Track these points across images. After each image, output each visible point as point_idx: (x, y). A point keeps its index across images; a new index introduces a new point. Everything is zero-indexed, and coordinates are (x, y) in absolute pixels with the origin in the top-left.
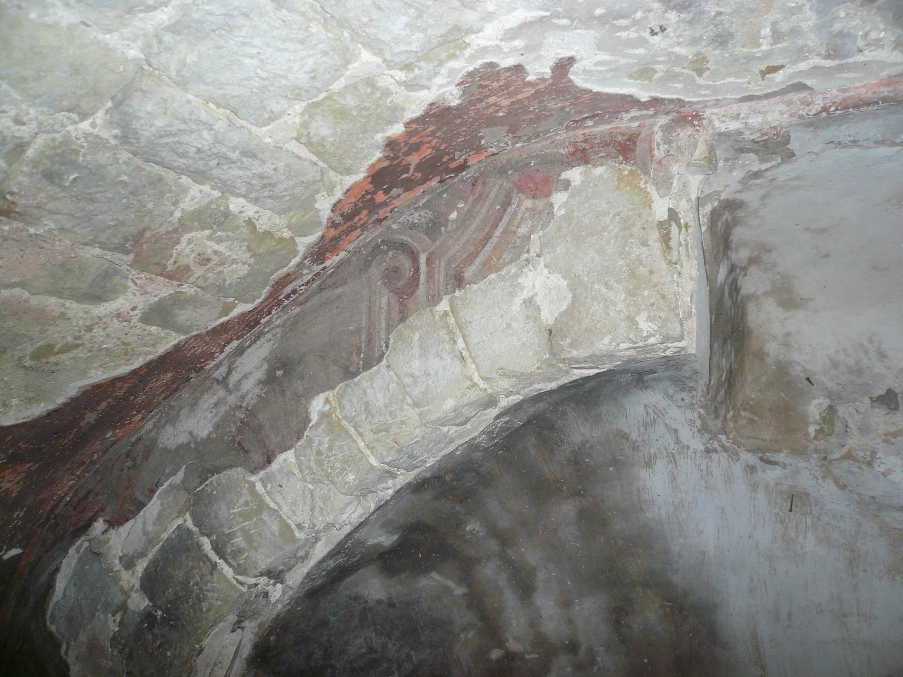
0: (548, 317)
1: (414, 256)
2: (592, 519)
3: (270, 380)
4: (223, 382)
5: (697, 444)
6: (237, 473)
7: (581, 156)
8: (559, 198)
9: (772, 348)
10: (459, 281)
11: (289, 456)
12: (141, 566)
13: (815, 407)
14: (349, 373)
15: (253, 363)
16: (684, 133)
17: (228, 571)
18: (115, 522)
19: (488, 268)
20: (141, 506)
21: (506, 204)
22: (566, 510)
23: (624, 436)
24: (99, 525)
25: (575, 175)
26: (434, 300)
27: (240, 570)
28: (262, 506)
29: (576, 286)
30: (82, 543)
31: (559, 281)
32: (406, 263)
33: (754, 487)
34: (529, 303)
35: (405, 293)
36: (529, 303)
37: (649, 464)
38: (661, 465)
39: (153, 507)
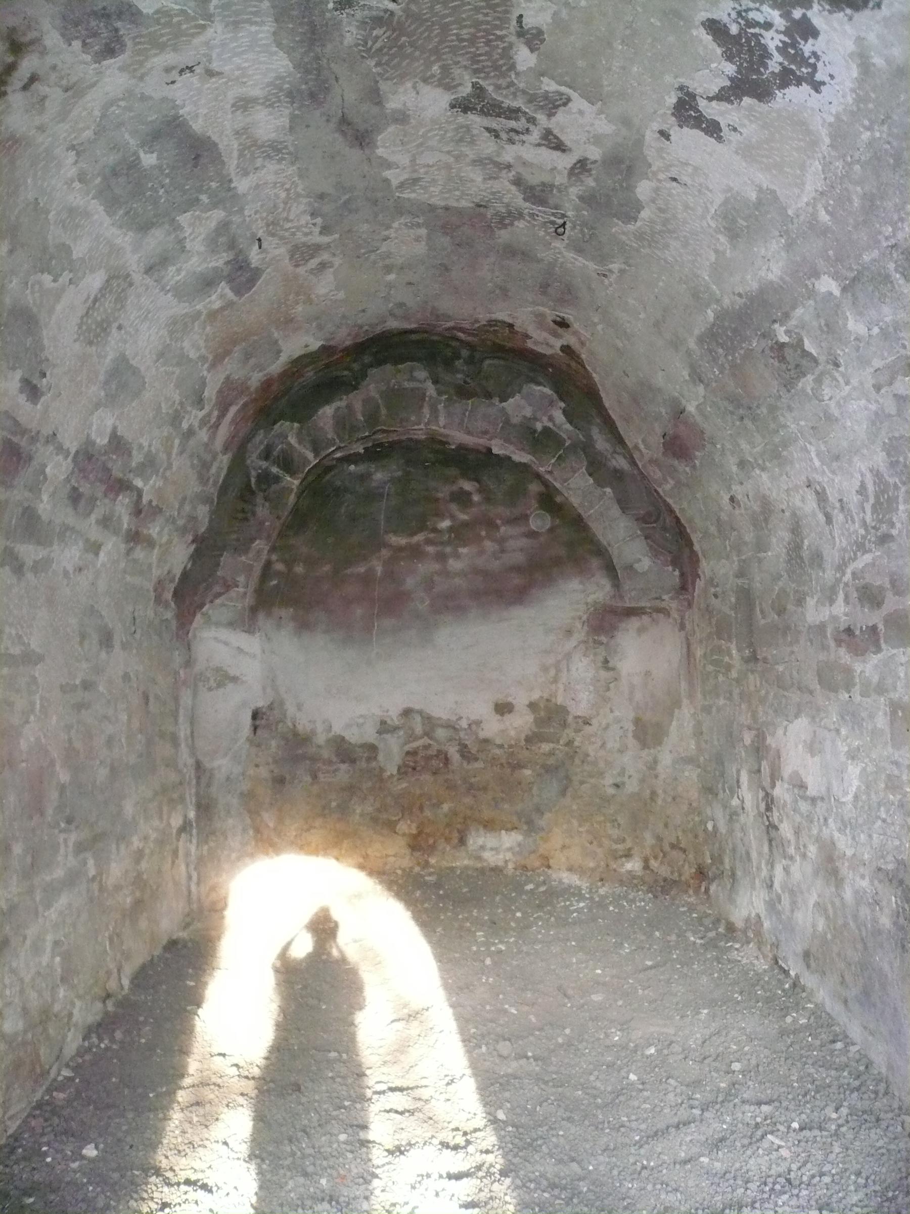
0: (636, 566)
1: (655, 522)
2: (557, 562)
3: (616, 471)
4: (615, 452)
5: (590, 599)
6: (585, 463)
7: (682, 575)
8: (670, 568)
9: (624, 625)
10: (646, 538)
11: (591, 481)
12: (550, 425)
13: (603, 639)
14: (619, 501)
15: (620, 462)
16: (686, 603)
17: (553, 461)
18: (565, 412)
19: (651, 547)
20: (571, 423)
21: (670, 552)
22: (562, 552)
23: (593, 576)
24: (563, 405)
25: (677, 573)
26: (642, 529)
27: (554, 464)
28: (575, 472)
29: (644, 574)
30: (555, 397)
31: (646, 568)
32: (654, 518)
33: (573, 618)
34: (640, 560)
35: (643, 520)
36: (640, 560)
37: (581, 582)
38: (581, 586)
39: (568, 426)
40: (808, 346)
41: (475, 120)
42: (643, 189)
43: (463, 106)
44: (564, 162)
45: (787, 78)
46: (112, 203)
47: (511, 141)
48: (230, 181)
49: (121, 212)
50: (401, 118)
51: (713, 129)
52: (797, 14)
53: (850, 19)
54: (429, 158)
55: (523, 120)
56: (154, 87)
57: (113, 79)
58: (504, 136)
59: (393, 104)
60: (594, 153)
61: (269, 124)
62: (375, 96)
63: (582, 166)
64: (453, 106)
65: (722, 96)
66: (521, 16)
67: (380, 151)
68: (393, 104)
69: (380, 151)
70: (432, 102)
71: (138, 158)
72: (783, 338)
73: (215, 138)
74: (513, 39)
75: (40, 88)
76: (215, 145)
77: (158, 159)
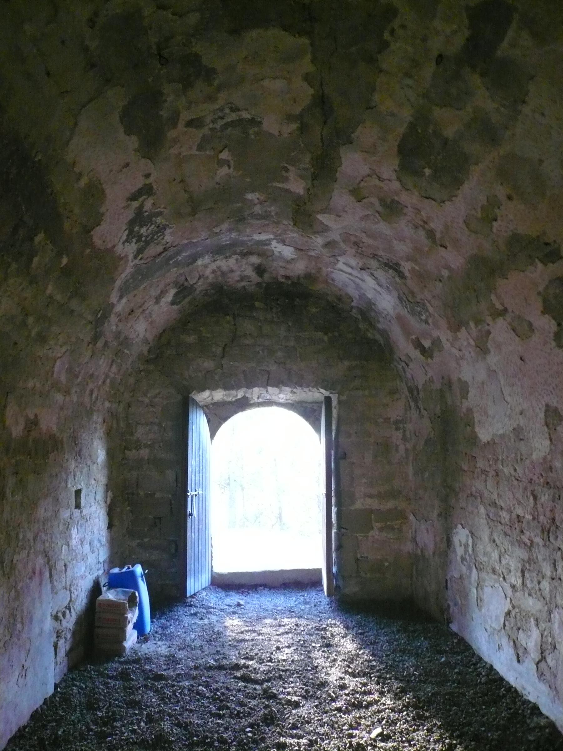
40: (36, 259)
41: (246, 115)
42: (133, 142)
43: (253, 122)
44: (185, 116)
45: (131, 232)
46: (458, 183)
47: (221, 109)
48: (411, 123)
49: (460, 175)
50: (290, 118)
51: (133, 198)
52: (143, 239)
53: (133, 253)
54: (279, 84)
55: (218, 127)
56: (396, 185)
57: (404, 198)
58: (227, 111)
59: (294, 126)
60: (171, 134)
61: (367, 133)
62: (303, 129)
63: (174, 121)
64: (260, 123)
65: (142, 206)
66: (229, 168)
67: (311, 91)
68: (294, 126)
69: (311, 91)
70: (271, 124)
71: (429, 175)
72: (37, 239)
73: (396, 149)
74: (230, 158)
75: (425, 219)
76: (398, 146)
77: (424, 168)
